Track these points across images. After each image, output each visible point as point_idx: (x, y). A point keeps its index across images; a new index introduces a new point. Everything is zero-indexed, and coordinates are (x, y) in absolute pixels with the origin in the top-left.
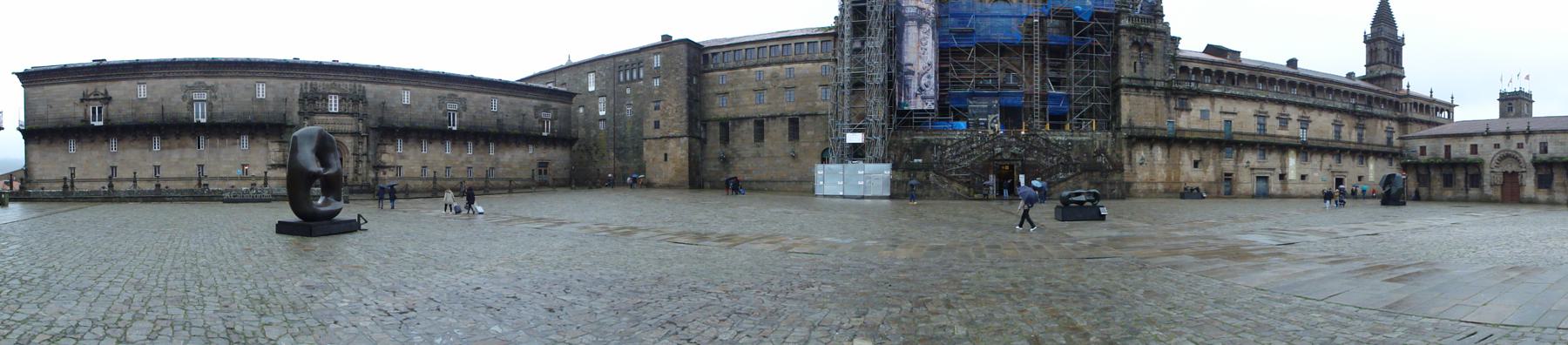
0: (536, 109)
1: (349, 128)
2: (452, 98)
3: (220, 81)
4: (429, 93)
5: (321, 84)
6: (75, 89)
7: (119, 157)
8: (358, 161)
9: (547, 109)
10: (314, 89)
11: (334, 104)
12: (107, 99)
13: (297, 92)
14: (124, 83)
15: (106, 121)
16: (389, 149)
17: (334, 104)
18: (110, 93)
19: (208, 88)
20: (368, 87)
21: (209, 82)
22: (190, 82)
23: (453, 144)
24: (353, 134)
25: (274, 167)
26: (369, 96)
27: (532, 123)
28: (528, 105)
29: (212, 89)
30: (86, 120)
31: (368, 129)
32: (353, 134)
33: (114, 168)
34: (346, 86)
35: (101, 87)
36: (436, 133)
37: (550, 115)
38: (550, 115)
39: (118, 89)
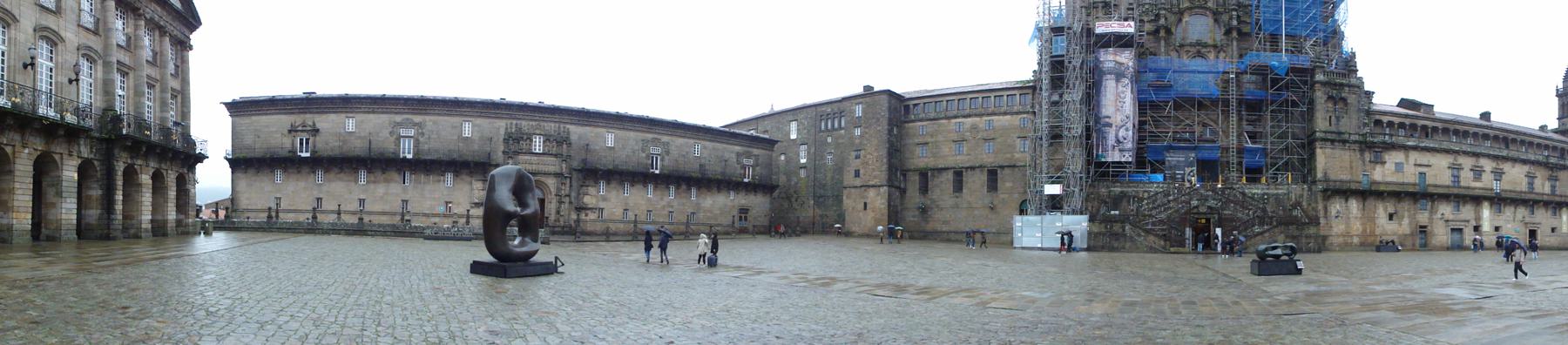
0: (738, 155)
1: (552, 169)
2: (655, 142)
3: (427, 118)
4: (633, 137)
5: (525, 125)
6: (284, 120)
7: (325, 188)
8: (561, 202)
9: (749, 156)
10: (519, 129)
11: (538, 145)
12: (315, 131)
13: (502, 131)
14: (333, 116)
15: (314, 152)
16: (592, 190)
17: (538, 145)
18: (318, 126)
19: (415, 124)
20: (572, 128)
21: (417, 119)
22: (398, 118)
23: (656, 188)
24: (558, 175)
25: (477, 205)
26: (574, 138)
27: (734, 170)
28: (731, 151)
29: (419, 125)
30: (293, 151)
31: (572, 170)
32: (558, 175)
33: (319, 200)
34: (551, 127)
35: (309, 119)
36: (640, 177)
37: (751, 162)
38: (751, 162)
39: (327, 123)
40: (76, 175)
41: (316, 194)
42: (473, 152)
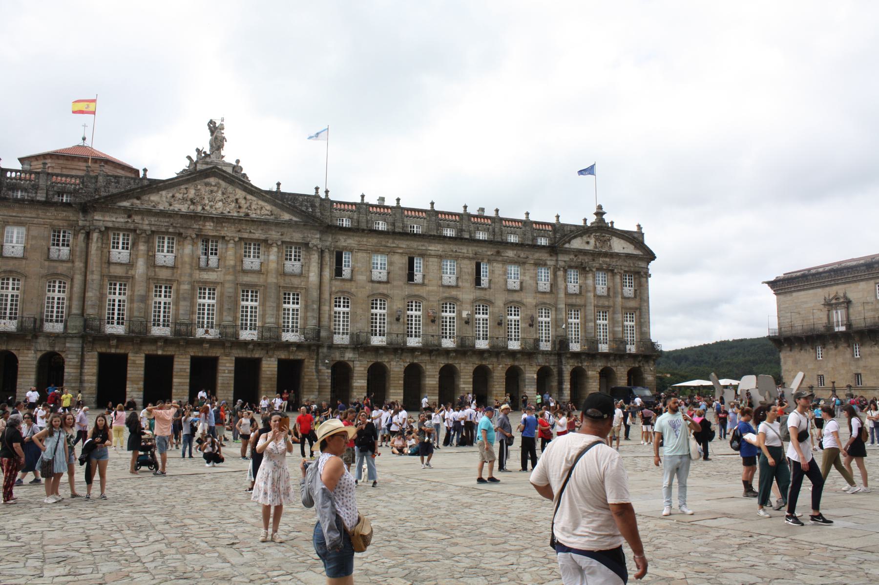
7: (862, 363)
12: (848, 303)
14: (862, 285)
18: (851, 296)
30: (829, 327)
33: (858, 375)
35: (838, 290)
39: (857, 291)
40: (535, 376)
41: (854, 369)
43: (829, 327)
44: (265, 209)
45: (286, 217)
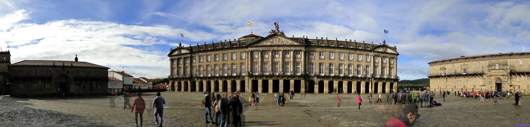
1: (502, 74)
21: (466, 63)
22: (462, 64)
30: (441, 74)
35: (444, 66)
42: (480, 70)
43: (441, 74)
44: (290, 42)
45: (296, 44)
